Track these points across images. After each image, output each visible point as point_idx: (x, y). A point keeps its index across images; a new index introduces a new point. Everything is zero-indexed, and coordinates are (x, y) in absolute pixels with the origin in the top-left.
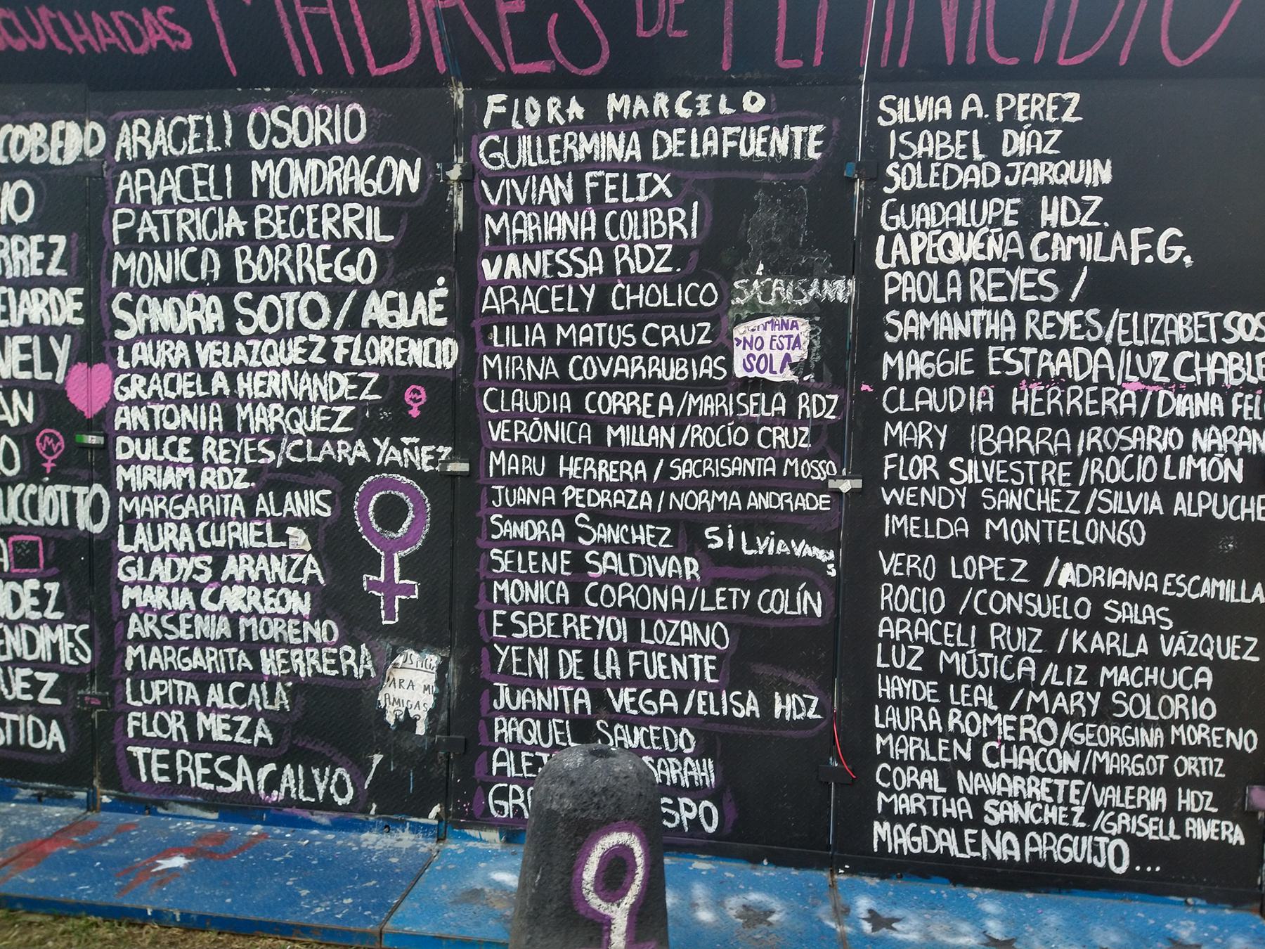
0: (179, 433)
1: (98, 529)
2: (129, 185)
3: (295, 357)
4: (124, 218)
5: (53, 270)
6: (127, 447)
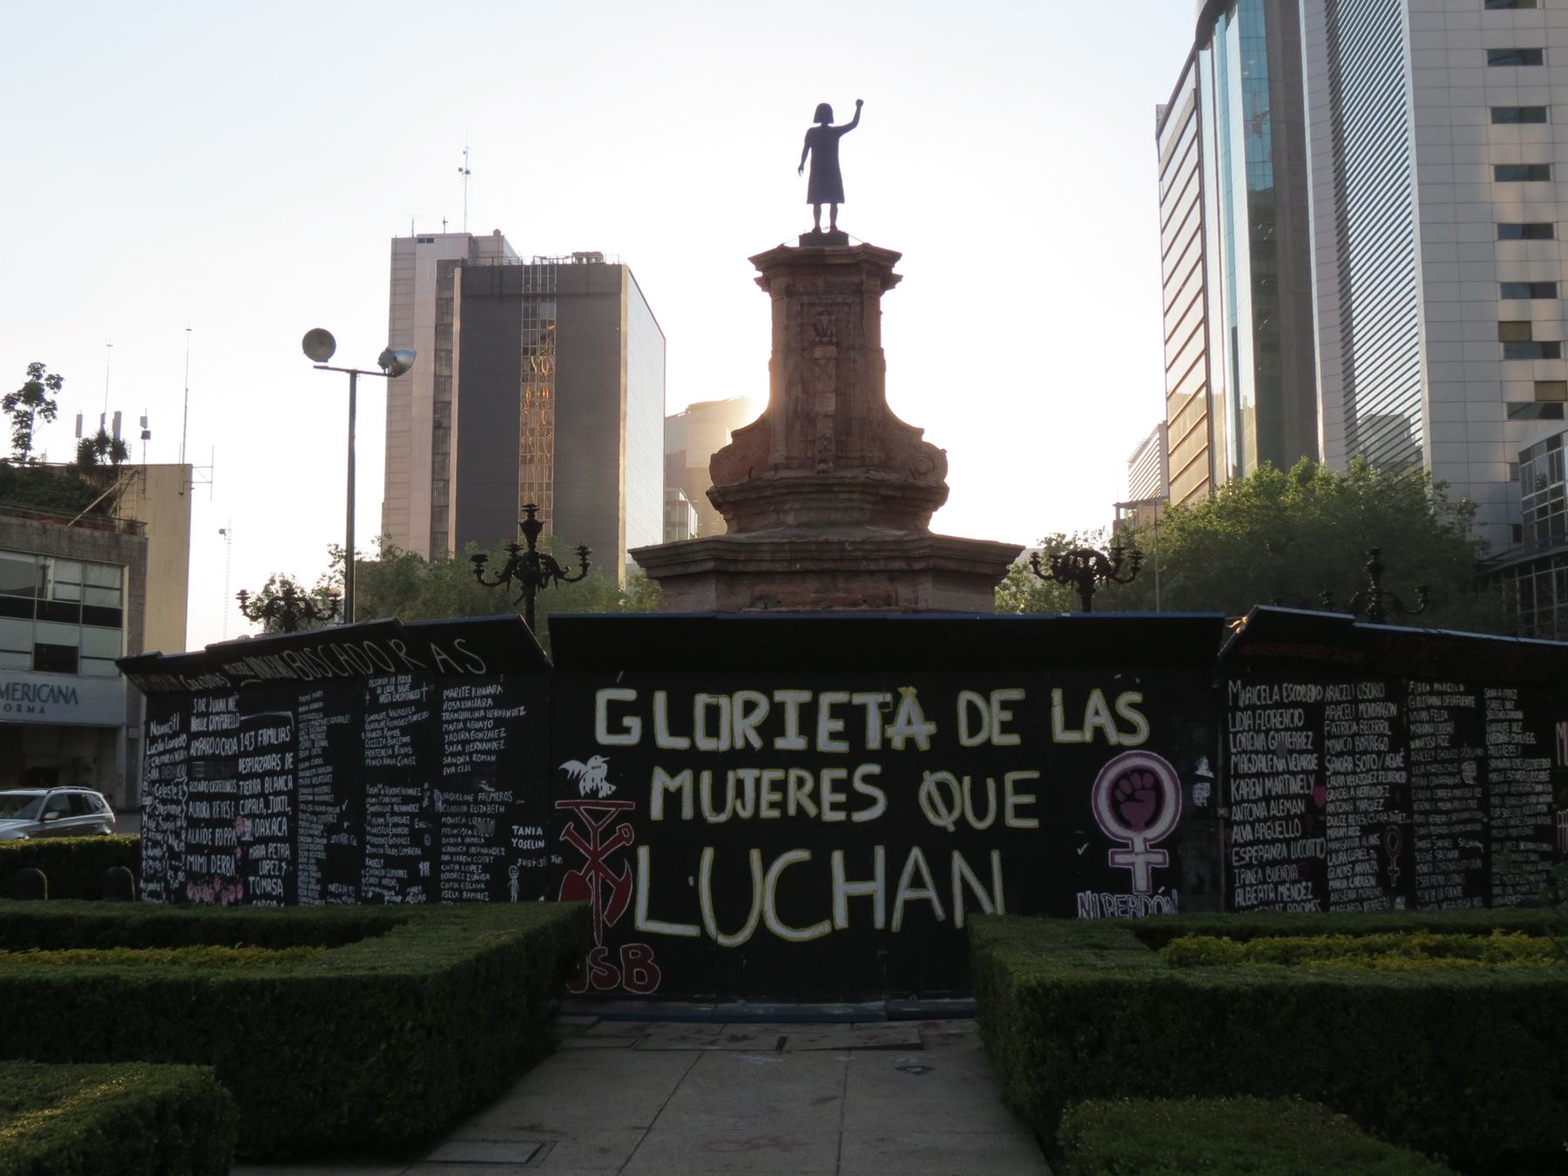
0: (1343, 813)
1: (1322, 857)
2: (1329, 712)
3: (1370, 782)
4: (1328, 725)
5: (1309, 747)
6: (1331, 821)
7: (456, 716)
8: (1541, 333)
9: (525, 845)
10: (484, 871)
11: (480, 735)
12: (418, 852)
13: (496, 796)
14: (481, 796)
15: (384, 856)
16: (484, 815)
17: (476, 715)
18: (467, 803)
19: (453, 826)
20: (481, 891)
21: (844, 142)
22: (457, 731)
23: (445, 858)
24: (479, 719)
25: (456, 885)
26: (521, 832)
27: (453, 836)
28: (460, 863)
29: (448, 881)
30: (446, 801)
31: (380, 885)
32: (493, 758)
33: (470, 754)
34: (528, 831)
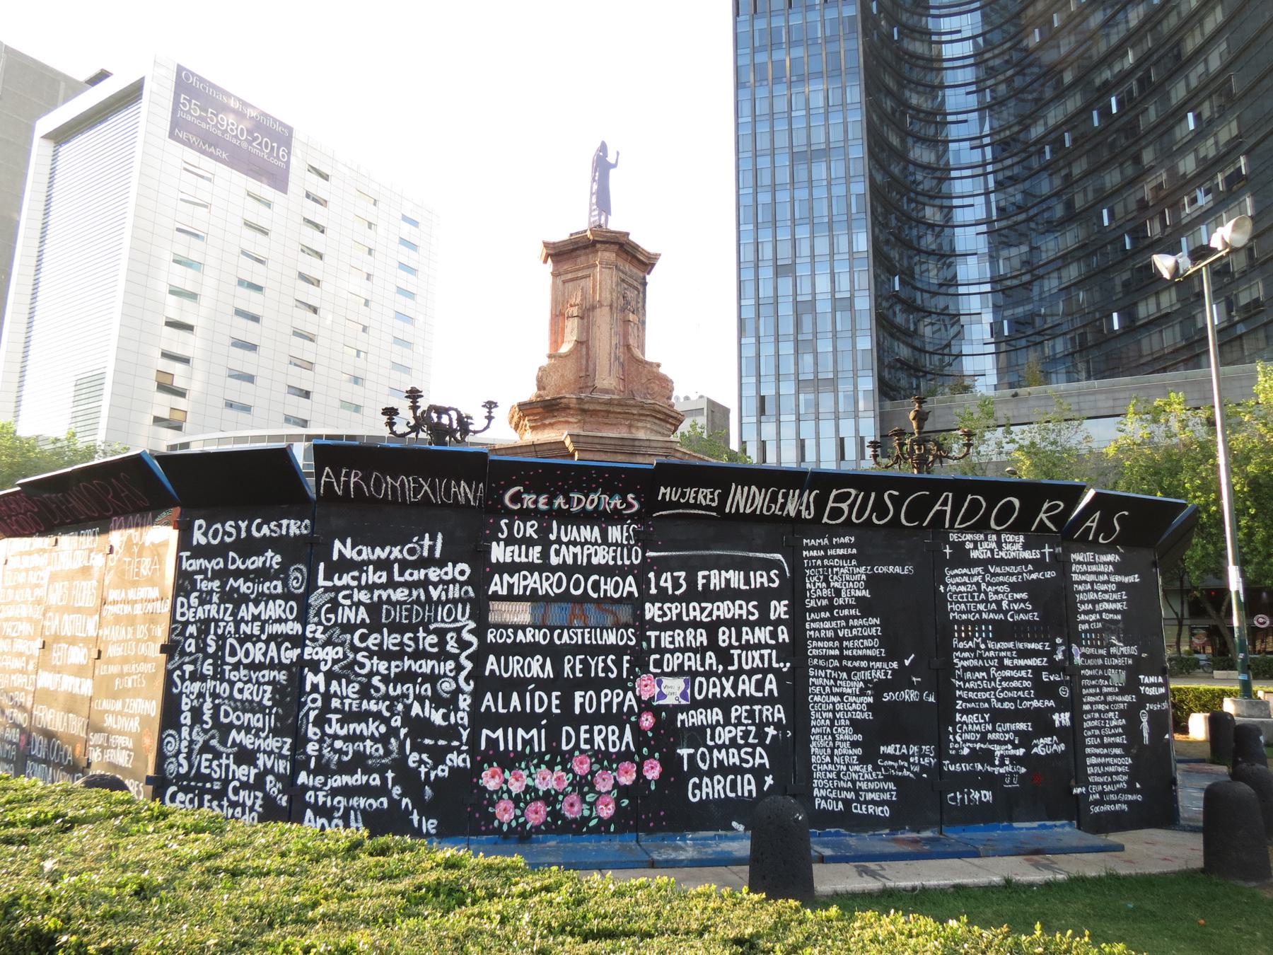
7: (1084, 578)
8: (178, 383)
9: (1151, 691)
10: (1121, 717)
11: (1107, 597)
12: (1051, 703)
13: (1124, 649)
14: (1113, 650)
15: (992, 710)
16: (1116, 667)
17: (1102, 578)
18: (1102, 657)
19: (1092, 678)
20: (1119, 735)
21: (612, 172)
22: (1086, 592)
23: (1086, 707)
24: (1104, 582)
25: (1097, 732)
26: (1146, 681)
27: (1093, 686)
28: (1099, 711)
29: (1089, 729)
30: (1083, 655)
31: (984, 739)
32: (1119, 617)
33: (1100, 613)
34: (1152, 679)
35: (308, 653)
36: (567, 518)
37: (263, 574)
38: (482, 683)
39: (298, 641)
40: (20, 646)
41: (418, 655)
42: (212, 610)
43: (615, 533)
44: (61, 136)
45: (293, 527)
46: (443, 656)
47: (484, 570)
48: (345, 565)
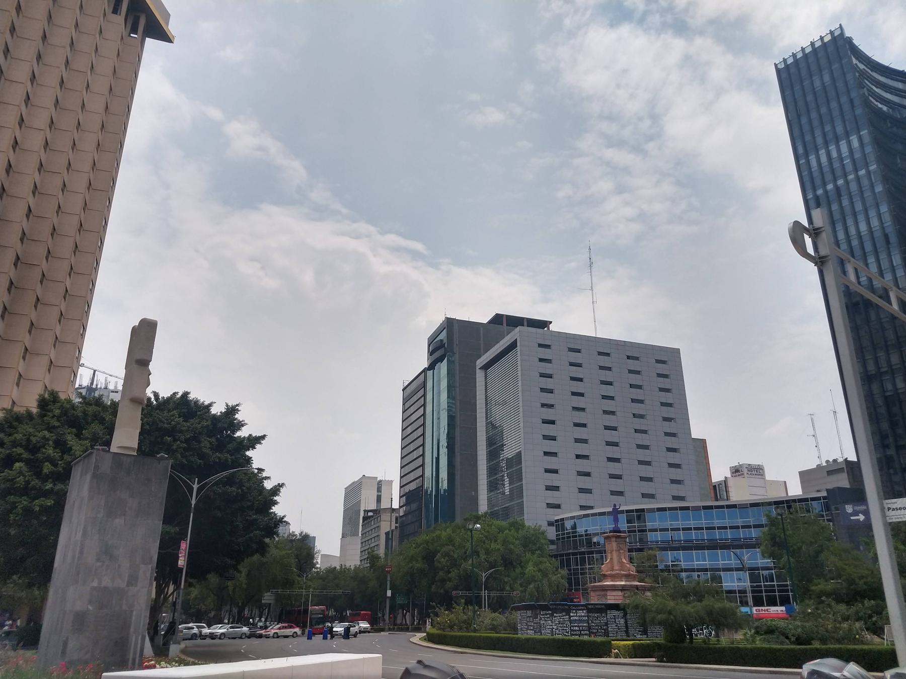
35: (553, 627)
36: (578, 610)
37: (548, 618)
38: (572, 630)
39: (552, 626)
40: (525, 627)
41: (564, 627)
42: (544, 622)
43: (584, 611)
44: (486, 367)
45: (550, 612)
46: (567, 627)
47: (570, 617)
48: (555, 617)
